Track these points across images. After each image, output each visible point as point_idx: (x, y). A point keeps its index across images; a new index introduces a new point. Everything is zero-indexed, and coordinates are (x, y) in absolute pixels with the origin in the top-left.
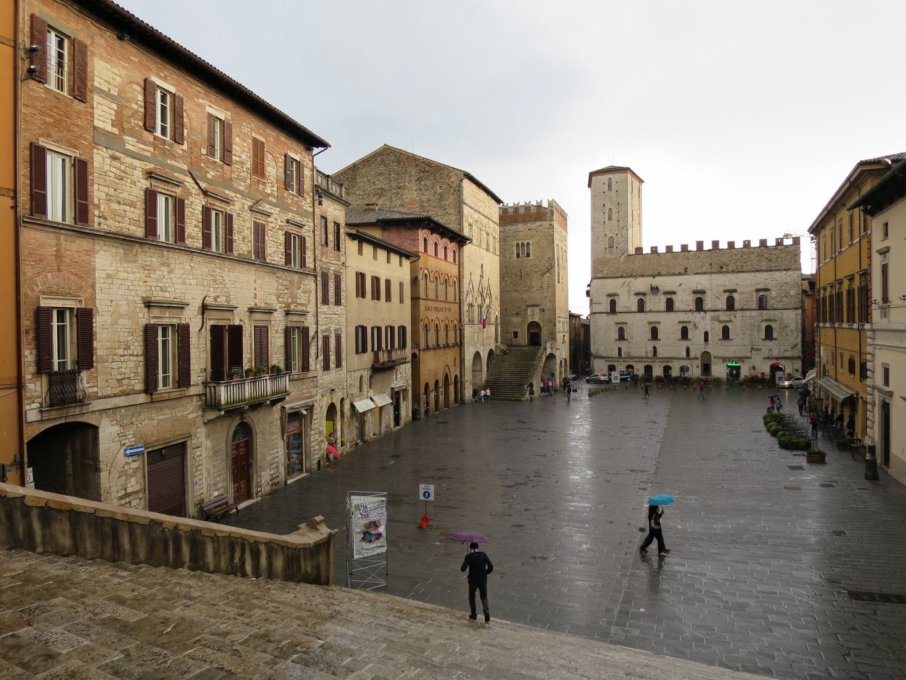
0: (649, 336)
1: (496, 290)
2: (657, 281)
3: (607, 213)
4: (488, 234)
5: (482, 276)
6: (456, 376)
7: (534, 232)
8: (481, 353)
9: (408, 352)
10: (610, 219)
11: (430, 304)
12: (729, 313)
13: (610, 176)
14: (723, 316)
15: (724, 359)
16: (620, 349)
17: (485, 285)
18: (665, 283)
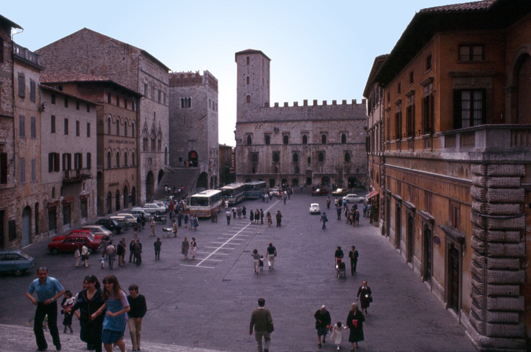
1: (165, 131)
2: (277, 126)
4: (160, 92)
5: (154, 120)
6: (134, 188)
8: (154, 172)
9: (94, 172)
10: (248, 83)
11: (112, 138)
13: (248, 55)
17: (157, 126)
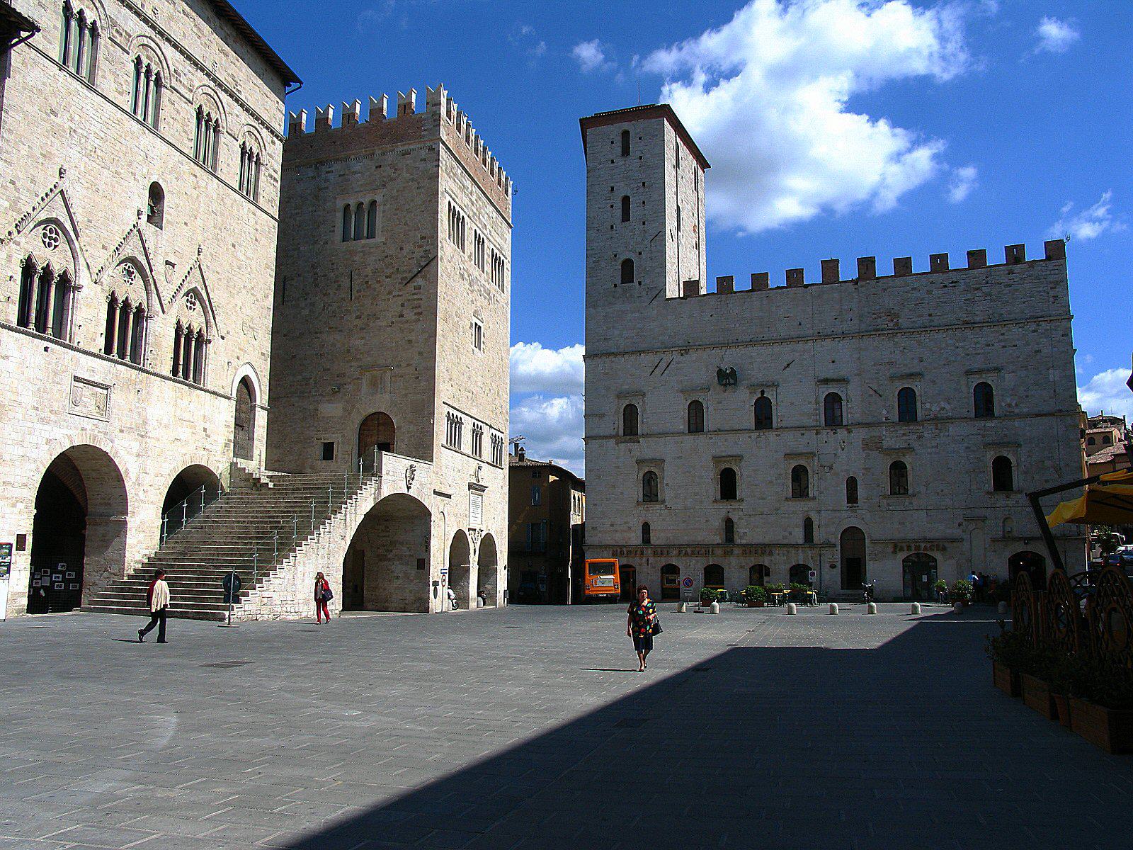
0: (714, 490)
3: (619, 205)
7: (390, 171)
10: (626, 217)
12: (902, 429)
13: (626, 126)
14: (891, 440)
15: (897, 546)
16: (646, 528)
18: (757, 363)
